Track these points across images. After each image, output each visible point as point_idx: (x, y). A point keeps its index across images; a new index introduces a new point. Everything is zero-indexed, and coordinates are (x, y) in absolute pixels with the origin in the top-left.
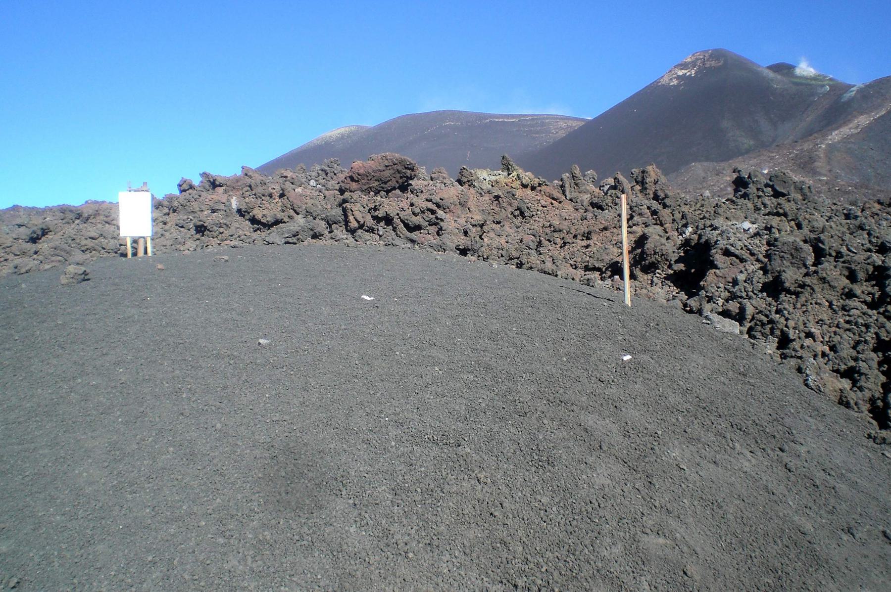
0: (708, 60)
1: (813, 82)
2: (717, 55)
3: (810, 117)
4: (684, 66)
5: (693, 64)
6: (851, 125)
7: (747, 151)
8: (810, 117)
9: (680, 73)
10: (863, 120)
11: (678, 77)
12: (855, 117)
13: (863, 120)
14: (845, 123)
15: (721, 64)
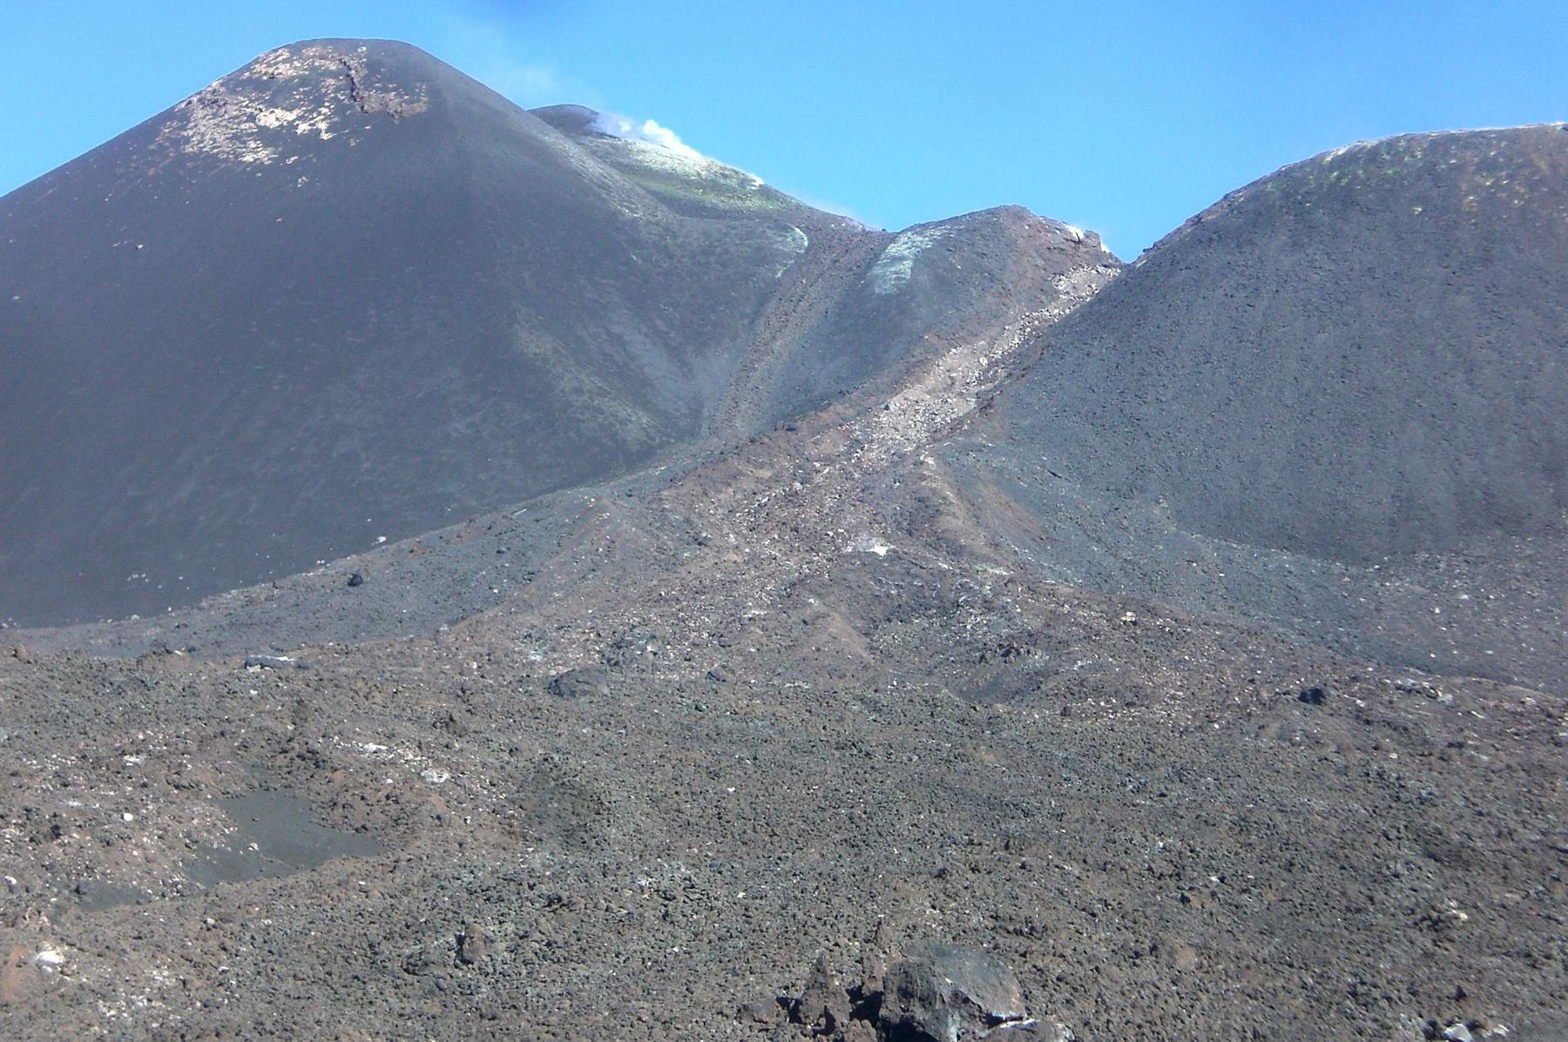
0: (368, 83)
1: (712, 199)
2: (394, 66)
3: (783, 342)
4: (253, 85)
5: (308, 91)
6: (931, 381)
7: (645, 455)
8: (783, 342)
9: (271, 119)
10: (962, 364)
11: (266, 136)
12: (937, 353)
13: (962, 364)
14: (912, 371)
15: (420, 107)
